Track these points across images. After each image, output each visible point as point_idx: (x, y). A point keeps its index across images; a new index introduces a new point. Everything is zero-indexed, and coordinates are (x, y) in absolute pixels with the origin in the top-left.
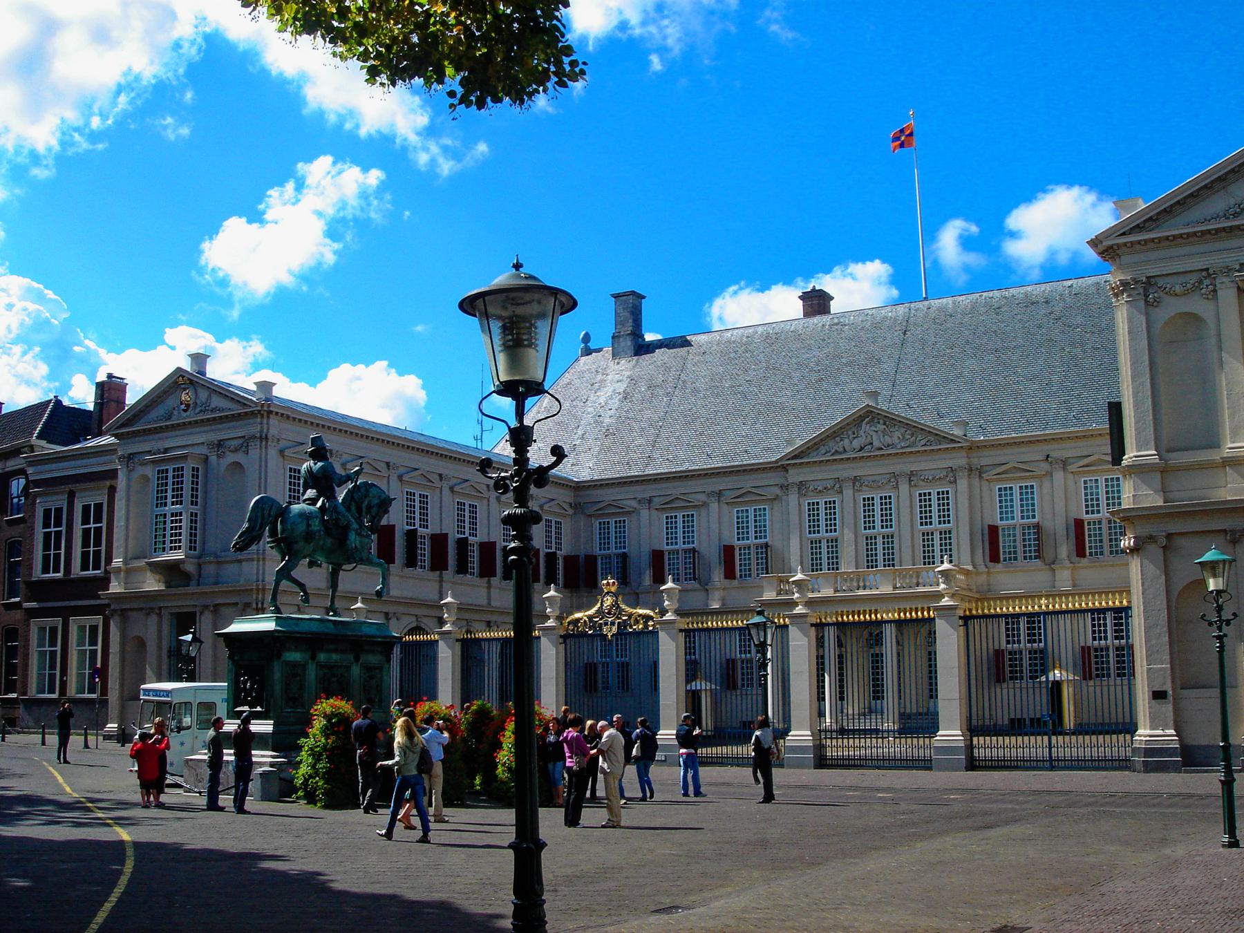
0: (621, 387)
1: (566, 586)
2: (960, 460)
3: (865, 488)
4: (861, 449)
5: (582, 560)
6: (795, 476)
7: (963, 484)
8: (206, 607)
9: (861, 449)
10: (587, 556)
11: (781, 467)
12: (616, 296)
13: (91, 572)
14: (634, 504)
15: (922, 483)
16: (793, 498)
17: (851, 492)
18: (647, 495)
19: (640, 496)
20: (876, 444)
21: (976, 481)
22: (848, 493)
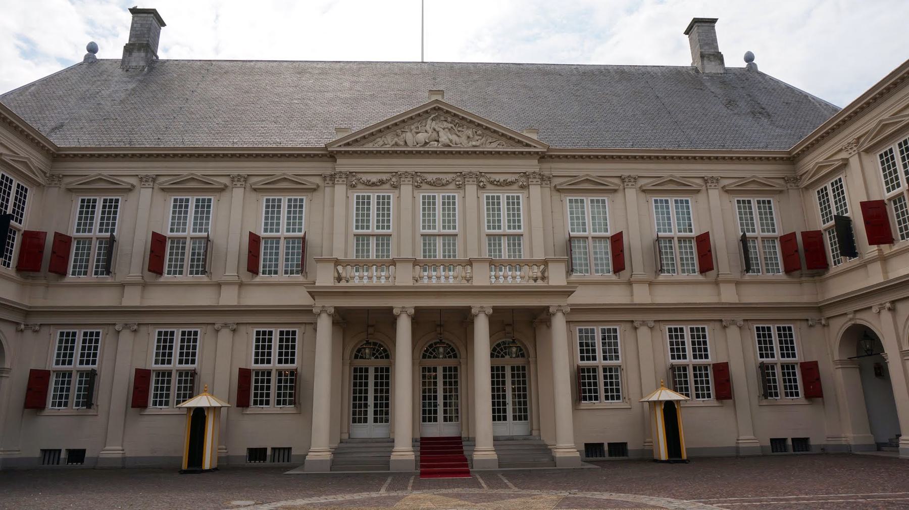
1: (20, 268)
2: (531, 166)
3: (424, 186)
4: (426, 143)
5: (50, 239)
6: (344, 165)
7: (535, 191)
9: (426, 143)
10: (57, 235)
11: (330, 155)
12: (134, 11)
14: (133, 181)
15: (489, 186)
16: (340, 190)
17: (410, 187)
18: (153, 173)
20: (444, 137)
21: (547, 191)
22: (406, 189)
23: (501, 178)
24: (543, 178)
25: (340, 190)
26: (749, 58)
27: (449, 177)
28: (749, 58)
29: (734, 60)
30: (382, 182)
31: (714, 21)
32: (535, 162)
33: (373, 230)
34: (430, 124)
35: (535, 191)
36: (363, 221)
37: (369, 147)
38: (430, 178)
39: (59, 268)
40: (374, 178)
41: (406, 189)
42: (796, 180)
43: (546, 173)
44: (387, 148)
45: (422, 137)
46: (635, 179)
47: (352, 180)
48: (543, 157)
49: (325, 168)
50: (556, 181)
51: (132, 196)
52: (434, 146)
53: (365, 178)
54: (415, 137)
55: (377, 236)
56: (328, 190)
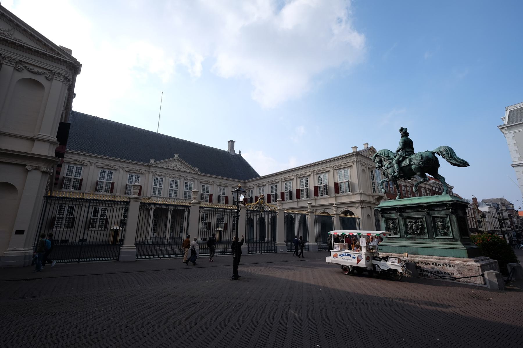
2: (196, 176)
6: (152, 169)
7: (196, 182)
16: (151, 175)
19: (91, 161)
22: (167, 178)
23: (189, 178)
24: (198, 180)
26: (240, 152)
28: (240, 152)
29: (237, 152)
31: (234, 142)
32: (197, 176)
34: (176, 163)
35: (196, 182)
36: (155, 184)
37: (159, 166)
38: (173, 176)
40: (160, 174)
41: (167, 178)
42: (245, 187)
44: (164, 167)
45: (173, 165)
47: (154, 173)
48: (199, 175)
49: (147, 169)
50: (201, 181)
52: (175, 168)
53: (158, 173)
54: (172, 165)
55: (159, 188)
56: (147, 175)
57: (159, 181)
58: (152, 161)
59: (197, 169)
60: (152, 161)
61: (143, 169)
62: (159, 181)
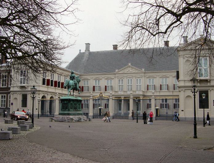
0: (87, 59)
2: (143, 74)
7: (143, 78)
8: (29, 93)
12: (86, 44)
13: (4, 87)
16: (116, 79)
25: (116, 79)
27: (131, 77)
30: (122, 78)
33: (121, 85)
34: (128, 69)
37: (120, 73)
38: (129, 77)
39: (83, 91)
40: (121, 77)
43: (145, 75)
46: (159, 76)
49: (114, 76)
50: (147, 76)
51: (90, 80)
54: (126, 71)
57: (121, 81)
58: (117, 71)
59: (143, 70)
60: (117, 71)
61: (112, 76)
62: (121, 81)
